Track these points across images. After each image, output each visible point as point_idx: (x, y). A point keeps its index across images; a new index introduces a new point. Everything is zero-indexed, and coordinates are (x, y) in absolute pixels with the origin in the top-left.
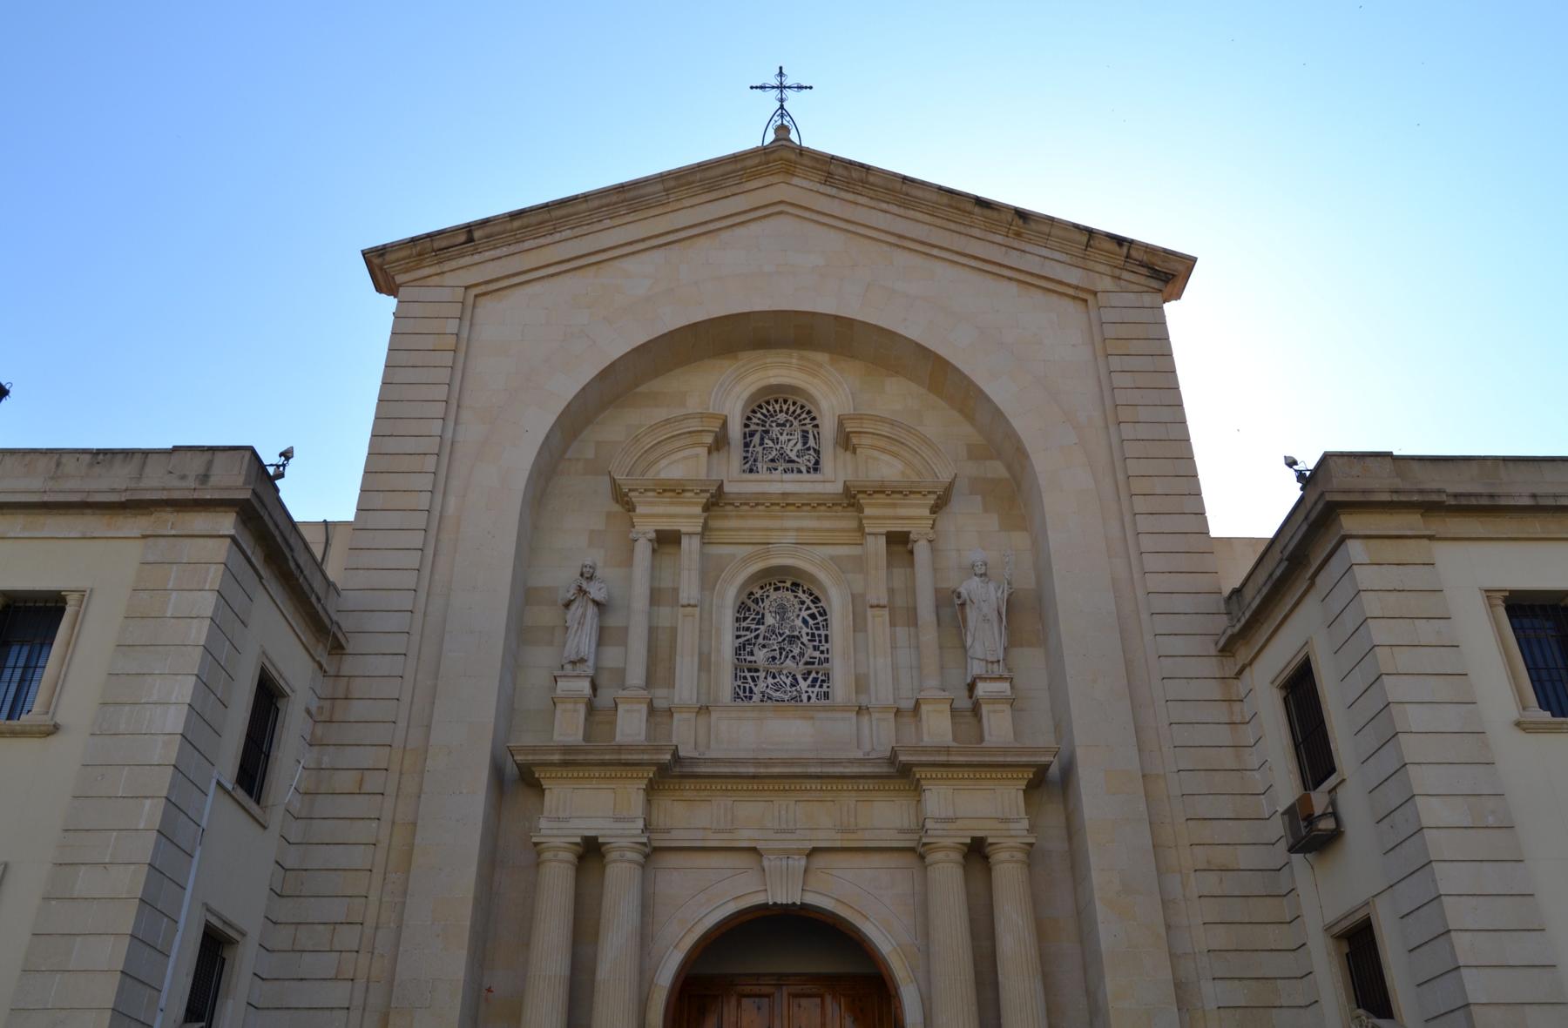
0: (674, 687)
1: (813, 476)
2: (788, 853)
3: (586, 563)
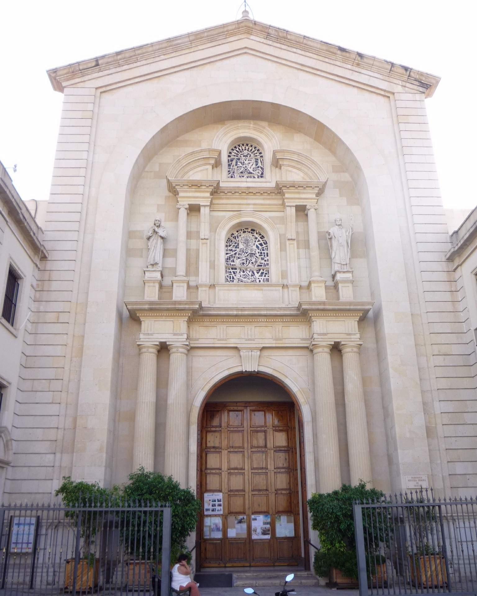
0: (198, 276)
1: (261, 179)
2: (252, 349)
3: (157, 219)
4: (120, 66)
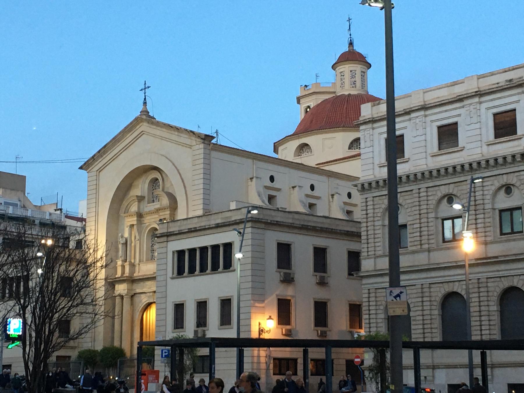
4: (102, 156)
